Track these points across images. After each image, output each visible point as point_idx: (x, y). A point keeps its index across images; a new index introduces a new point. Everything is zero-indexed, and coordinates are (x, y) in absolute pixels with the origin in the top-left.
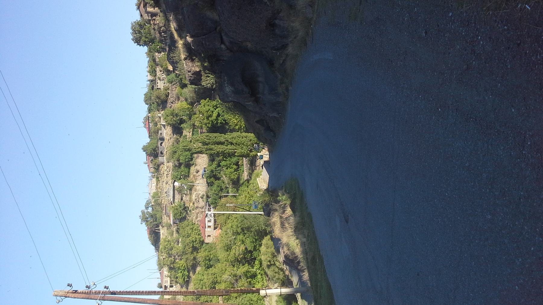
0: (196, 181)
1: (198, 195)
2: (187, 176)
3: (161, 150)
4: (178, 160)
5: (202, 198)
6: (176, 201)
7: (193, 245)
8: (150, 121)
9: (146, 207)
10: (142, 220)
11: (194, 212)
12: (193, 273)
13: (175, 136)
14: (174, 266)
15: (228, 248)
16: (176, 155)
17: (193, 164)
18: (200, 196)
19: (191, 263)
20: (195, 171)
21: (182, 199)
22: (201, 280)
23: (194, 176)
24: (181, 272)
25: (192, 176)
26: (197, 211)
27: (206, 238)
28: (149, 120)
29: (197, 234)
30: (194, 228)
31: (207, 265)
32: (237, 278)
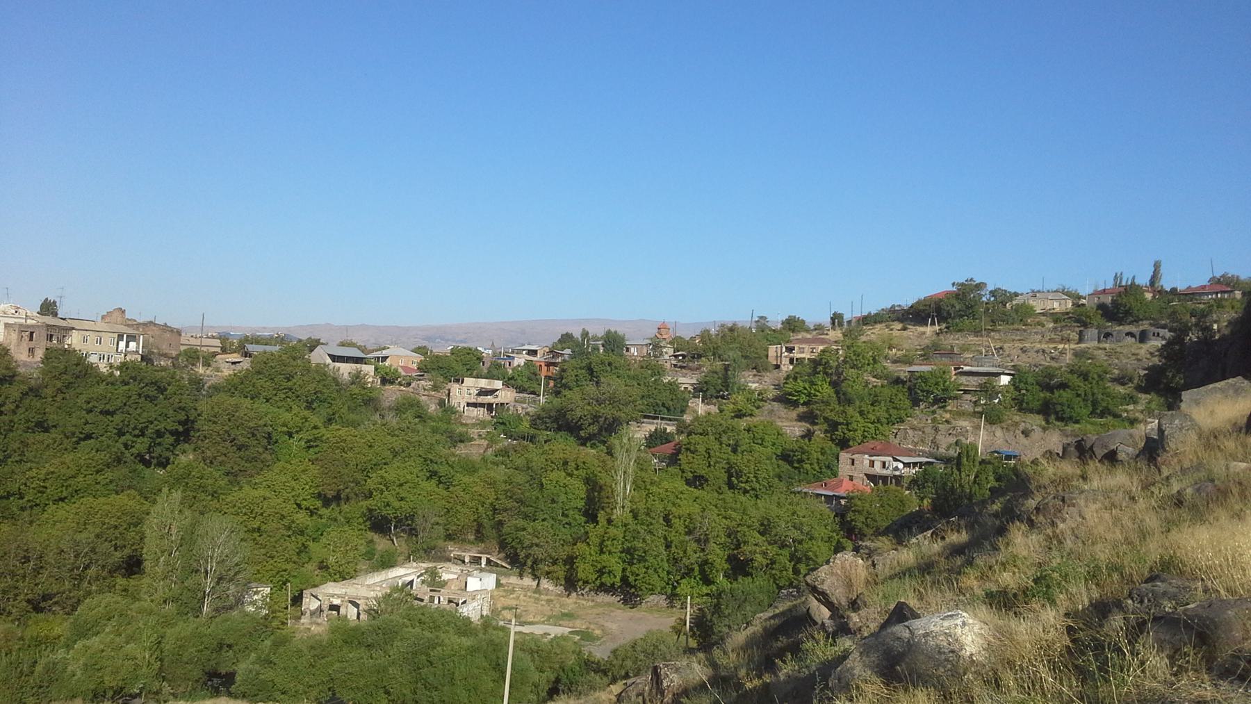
0: (1003, 428)
1: (964, 433)
2: (1021, 405)
3: (1114, 334)
4: (1063, 386)
5: (956, 443)
6: (963, 379)
7: (842, 423)
8: (1219, 296)
9: (996, 290)
10: (962, 284)
11: (930, 421)
12: (803, 413)
13: (1143, 373)
14: (819, 373)
15: (765, 528)
16: (1075, 381)
17: (1047, 422)
18: (961, 438)
19: (818, 412)
20: (1028, 426)
21: (966, 392)
22: (763, 440)
23: (1016, 424)
24: (805, 388)
25: (1017, 418)
26: (928, 430)
27: (849, 455)
28: (1223, 292)
29: (866, 433)
30: (882, 425)
31: (792, 454)
32: (703, 542)
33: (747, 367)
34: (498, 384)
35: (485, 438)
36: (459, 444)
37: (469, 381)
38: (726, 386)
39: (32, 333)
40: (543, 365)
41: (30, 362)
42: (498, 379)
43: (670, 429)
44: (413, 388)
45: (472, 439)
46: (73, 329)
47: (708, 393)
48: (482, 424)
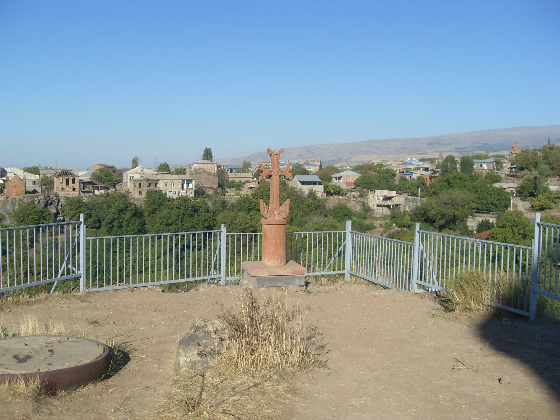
33: (554, 175)
34: (393, 193)
35: (383, 227)
36: (367, 231)
37: (378, 192)
38: (535, 188)
39: (140, 184)
40: (428, 178)
41: (140, 198)
42: (393, 190)
43: (492, 220)
44: (348, 197)
45: (375, 228)
46: (159, 180)
47: (523, 195)
48: (384, 217)
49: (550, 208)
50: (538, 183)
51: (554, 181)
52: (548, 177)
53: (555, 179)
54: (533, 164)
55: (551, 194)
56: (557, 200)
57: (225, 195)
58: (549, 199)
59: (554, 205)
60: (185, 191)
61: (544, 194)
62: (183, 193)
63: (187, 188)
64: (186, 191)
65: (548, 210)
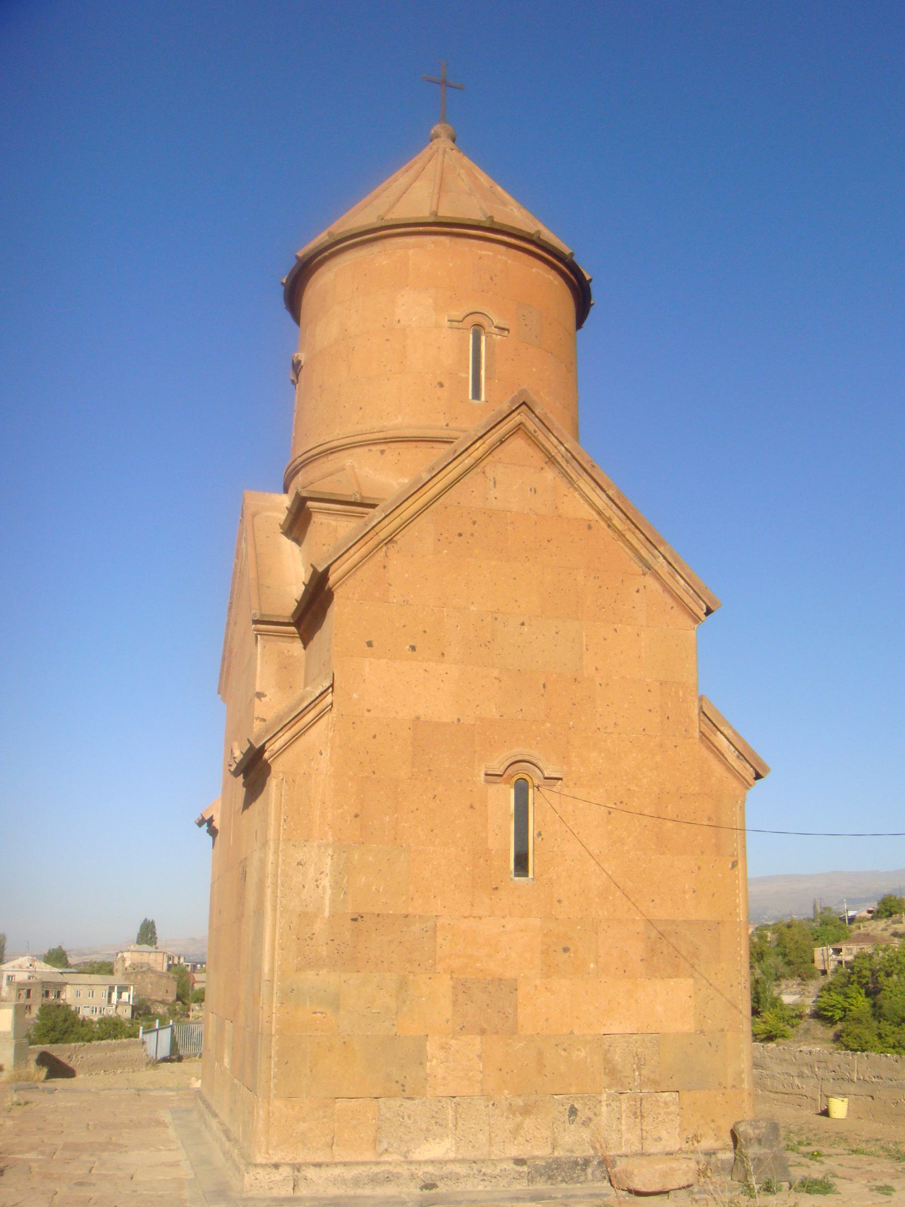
14: (852, 984)
33: (792, 975)
46: (67, 984)
49: (783, 1036)
50: (760, 989)
51: (792, 986)
52: (781, 979)
53: (794, 982)
54: (755, 955)
55: (785, 1009)
56: (795, 1021)
57: (188, 1016)
58: (782, 1019)
59: (791, 1030)
60: (114, 1007)
61: (772, 1010)
62: (110, 1011)
63: (117, 1002)
64: (117, 1007)
65: (780, 1040)
